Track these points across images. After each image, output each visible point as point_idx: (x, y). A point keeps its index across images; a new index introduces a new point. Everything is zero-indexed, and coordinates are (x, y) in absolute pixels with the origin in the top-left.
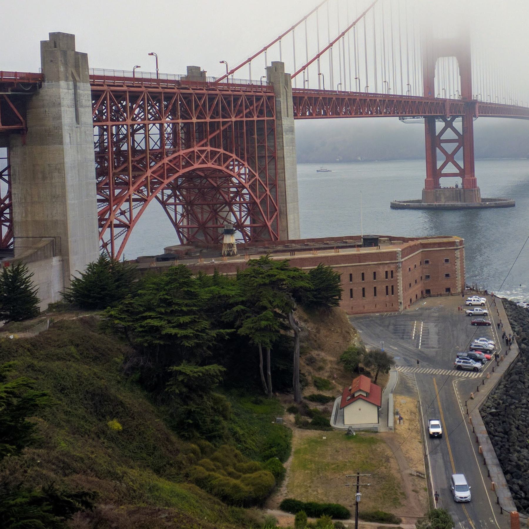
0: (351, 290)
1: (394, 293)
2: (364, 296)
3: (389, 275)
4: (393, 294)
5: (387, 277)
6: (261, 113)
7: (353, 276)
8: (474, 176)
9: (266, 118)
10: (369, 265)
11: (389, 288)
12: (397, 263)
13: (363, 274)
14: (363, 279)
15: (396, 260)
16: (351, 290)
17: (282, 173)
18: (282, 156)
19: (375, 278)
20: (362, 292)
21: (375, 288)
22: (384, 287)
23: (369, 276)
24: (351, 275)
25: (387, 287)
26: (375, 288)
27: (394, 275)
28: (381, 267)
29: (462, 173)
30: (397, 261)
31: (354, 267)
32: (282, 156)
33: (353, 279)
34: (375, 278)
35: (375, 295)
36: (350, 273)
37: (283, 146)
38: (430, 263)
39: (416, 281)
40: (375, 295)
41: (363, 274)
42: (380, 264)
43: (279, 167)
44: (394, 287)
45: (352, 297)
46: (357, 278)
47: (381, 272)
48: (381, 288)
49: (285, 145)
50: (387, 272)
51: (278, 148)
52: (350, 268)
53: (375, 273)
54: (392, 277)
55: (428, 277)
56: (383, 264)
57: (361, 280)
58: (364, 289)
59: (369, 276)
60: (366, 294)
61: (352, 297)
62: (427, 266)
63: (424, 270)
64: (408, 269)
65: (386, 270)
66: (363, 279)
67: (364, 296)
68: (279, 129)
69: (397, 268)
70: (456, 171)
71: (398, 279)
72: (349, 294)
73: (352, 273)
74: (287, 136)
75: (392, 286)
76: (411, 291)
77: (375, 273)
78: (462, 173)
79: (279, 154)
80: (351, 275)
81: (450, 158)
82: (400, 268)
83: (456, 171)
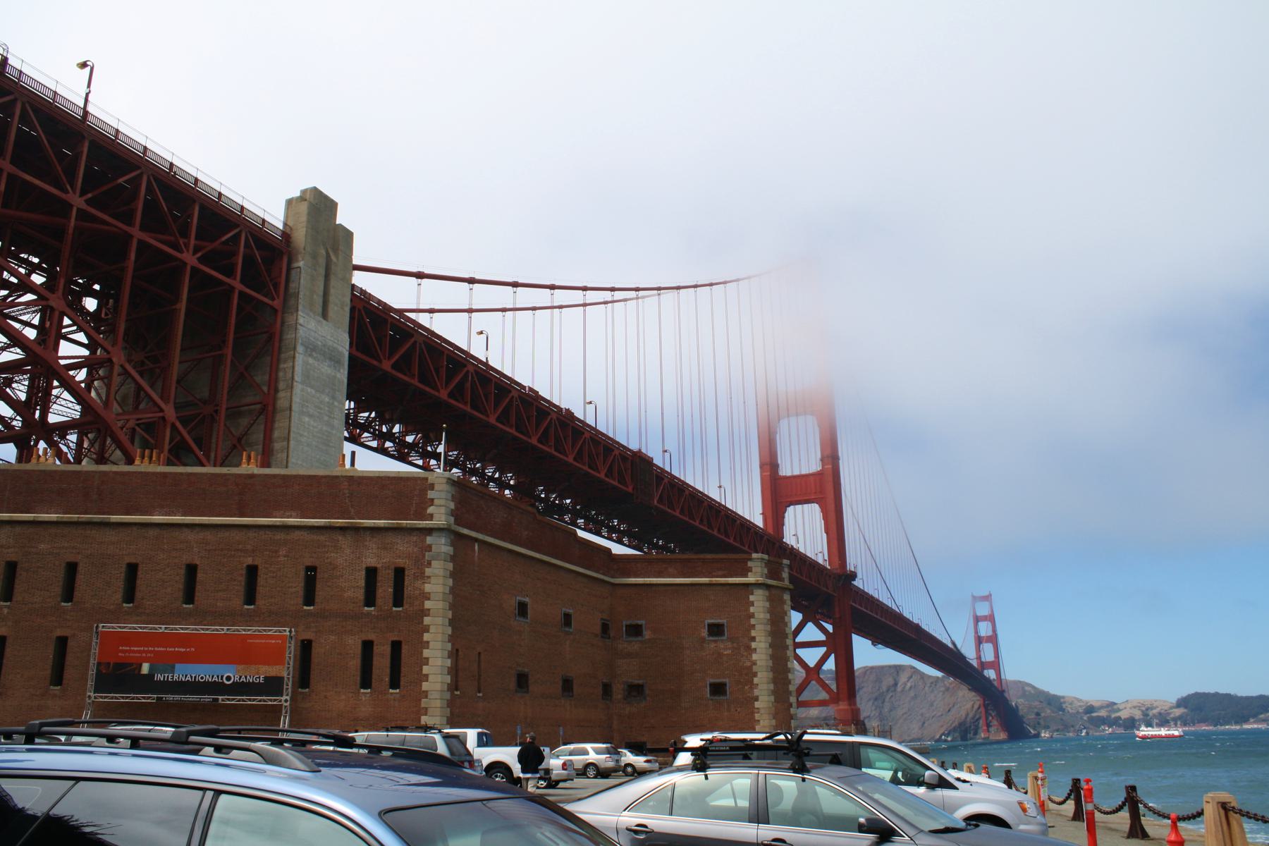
1: (403, 681)
3: (385, 590)
4: (395, 683)
5: (370, 599)
7: (200, 576)
8: (855, 704)
11: (377, 649)
12: (430, 531)
13: (252, 571)
15: (422, 515)
17: (282, 452)
19: (309, 599)
22: (354, 644)
24: (192, 570)
25: (368, 646)
27: (408, 590)
29: (834, 699)
31: (208, 535)
32: (288, 405)
34: (309, 599)
36: (186, 558)
38: (647, 634)
41: (252, 571)
42: (343, 529)
43: (276, 434)
44: (405, 649)
50: (371, 573)
51: (281, 385)
52: (191, 536)
54: (398, 599)
55: (635, 690)
56: (357, 529)
57: (237, 601)
62: (634, 645)
64: (511, 603)
65: (371, 561)
68: (289, 336)
70: (823, 695)
71: (426, 613)
74: (311, 361)
75: (396, 646)
78: (834, 699)
79: (282, 402)
80: (192, 570)
81: (814, 673)
83: (823, 695)
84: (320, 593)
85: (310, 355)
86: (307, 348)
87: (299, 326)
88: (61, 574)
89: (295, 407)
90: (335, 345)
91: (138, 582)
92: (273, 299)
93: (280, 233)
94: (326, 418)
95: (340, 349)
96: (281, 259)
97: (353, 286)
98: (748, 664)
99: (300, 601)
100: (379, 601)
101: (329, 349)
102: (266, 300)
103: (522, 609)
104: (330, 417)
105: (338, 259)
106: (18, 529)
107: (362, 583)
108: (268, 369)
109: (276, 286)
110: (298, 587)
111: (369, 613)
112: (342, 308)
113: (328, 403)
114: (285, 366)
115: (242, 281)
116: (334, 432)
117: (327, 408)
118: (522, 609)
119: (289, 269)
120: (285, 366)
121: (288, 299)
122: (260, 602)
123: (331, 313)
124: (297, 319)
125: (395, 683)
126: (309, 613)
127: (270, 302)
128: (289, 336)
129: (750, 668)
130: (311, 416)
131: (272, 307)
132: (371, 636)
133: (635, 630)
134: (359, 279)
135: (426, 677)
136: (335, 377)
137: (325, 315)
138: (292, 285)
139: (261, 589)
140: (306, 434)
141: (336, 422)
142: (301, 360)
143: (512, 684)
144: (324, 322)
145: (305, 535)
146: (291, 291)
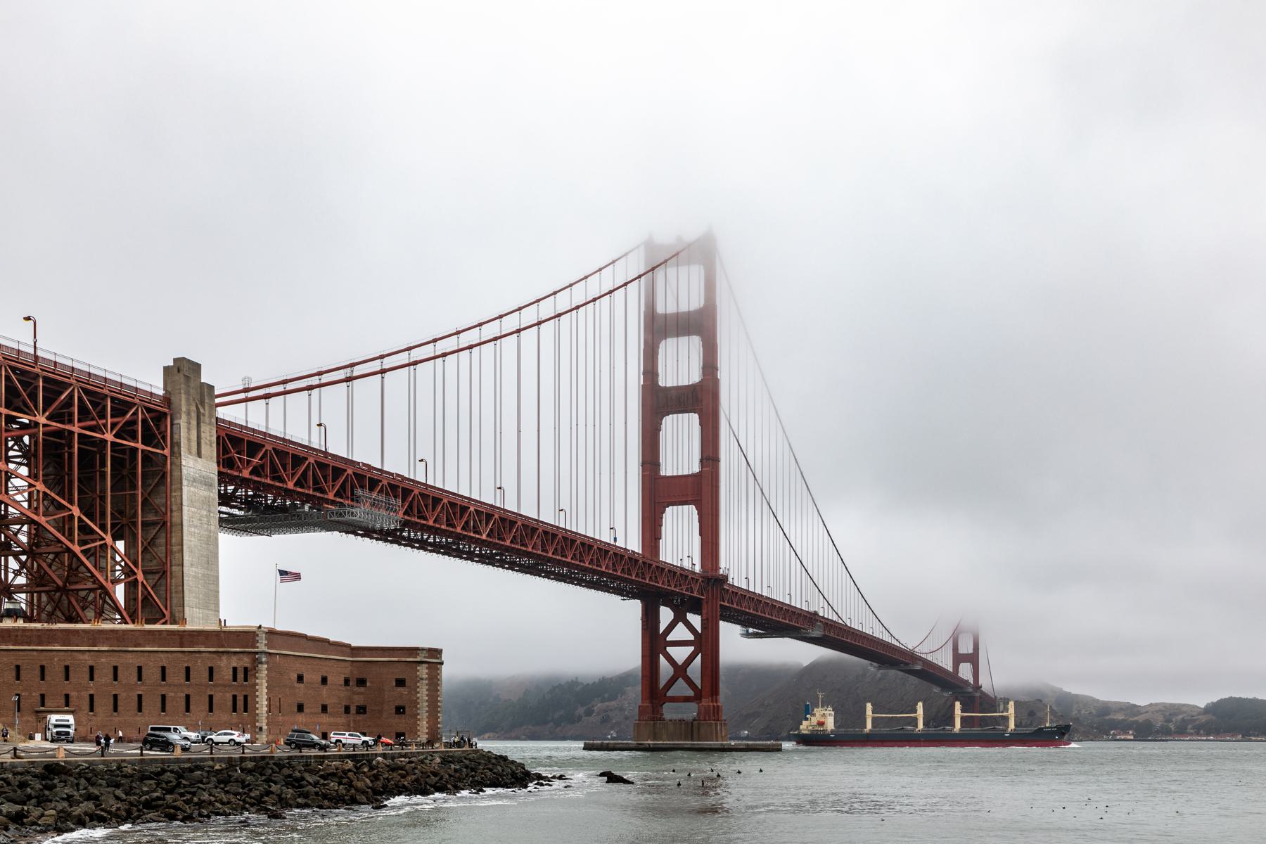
0: (164, 697)
1: (249, 710)
2: (188, 710)
3: (240, 676)
4: (246, 710)
5: (235, 679)
6: (127, 431)
9: (140, 446)
10: (199, 652)
13: (188, 669)
14: (188, 679)
16: (164, 697)
18: (178, 521)
19: (211, 679)
20: (183, 703)
21: (211, 697)
22: (229, 696)
23: (200, 674)
25: (235, 697)
26: (211, 697)
28: (224, 658)
30: (256, 650)
33: (167, 679)
34: (211, 679)
35: (211, 710)
37: (182, 504)
39: (324, 709)
40: (211, 710)
41: (188, 669)
42: (223, 652)
44: (249, 699)
45: (163, 710)
46: (176, 677)
47: (225, 666)
48: (223, 698)
49: (185, 503)
50: (235, 669)
53: (211, 670)
54: (246, 680)
56: (228, 652)
57: (183, 680)
58: (188, 697)
59: (200, 674)
60: (192, 707)
61: (163, 710)
63: (356, 697)
65: (235, 665)
66: (188, 679)
67: (188, 710)
69: (256, 662)
72: (159, 704)
73: (165, 665)
75: (246, 697)
76: (300, 718)
77: (211, 670)
79: (176, 520)
82: (261, 663)
84: (215, 677)
85: (192, 485)
86: (189, 481)
87: (183, 467)
88: (112, 670)
89: (185, 523)
90: (208, 474)
91: (143, 673)
92: (163, 449)
93: (162, 398)
94: (206, 526)
95: (211, 475)
96: (166, 418)
97: (217, 418)
98: (415, 698)
99: (208, 680)
100: (238, 680)
101: (204, 478)
102: (158, 451)
103: (300, 678)
104: (208, 525)
105: (204, 410)
106: (92, 653)
107: (231, 673)
108: (164, 495)
109: (164, 438)
110: (206, 674)
111: (234, 685)
112: (211, 446)
113: (206, 515)
114: (176, 494)
115: (142, 443)
116: (212, 534)
117: (205, 519)
118: (300, 678)
119: (172, 425)
120: (176, 494)
121: (176, 453)
122: (191, 681)
123: (203, 452)
124: (181, 462)
125: (246, 710)
126: (212, 685)
127: (161, 452)
128: (176, 474)
129: (416, 700)
130: (196, 527)
131: (163, 455)
132: (236, 694)
133: (361, 682)
134: (222, 413)
135: (258, 709)
136: (210, 496)
137: (199, 454)
138: (176, 436)
139: (192, 676)
140: (193, 539)
141: (212, 528)
142: (187, 491)
143: (296, 709)
144: (199, 459)
145: (208, 655)
146: (175, 441)
